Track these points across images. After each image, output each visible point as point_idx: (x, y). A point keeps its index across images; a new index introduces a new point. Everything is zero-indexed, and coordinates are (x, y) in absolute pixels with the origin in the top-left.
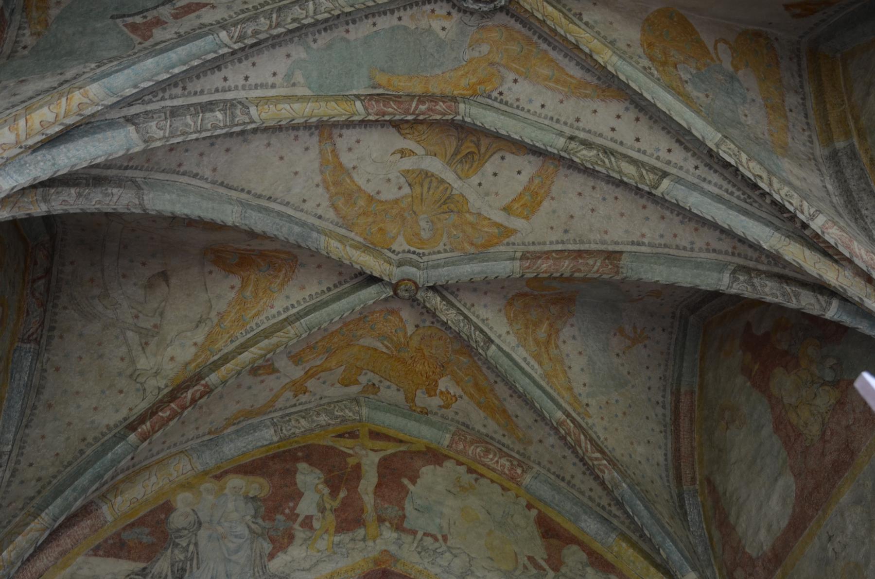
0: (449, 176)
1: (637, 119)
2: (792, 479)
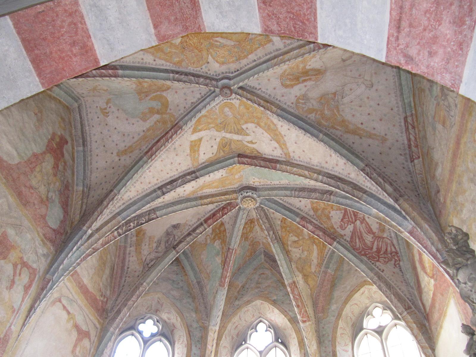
0: (228, 136)
1: (179, 195)
2: (16, 162)
